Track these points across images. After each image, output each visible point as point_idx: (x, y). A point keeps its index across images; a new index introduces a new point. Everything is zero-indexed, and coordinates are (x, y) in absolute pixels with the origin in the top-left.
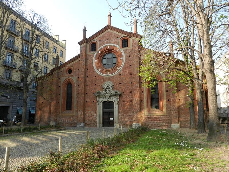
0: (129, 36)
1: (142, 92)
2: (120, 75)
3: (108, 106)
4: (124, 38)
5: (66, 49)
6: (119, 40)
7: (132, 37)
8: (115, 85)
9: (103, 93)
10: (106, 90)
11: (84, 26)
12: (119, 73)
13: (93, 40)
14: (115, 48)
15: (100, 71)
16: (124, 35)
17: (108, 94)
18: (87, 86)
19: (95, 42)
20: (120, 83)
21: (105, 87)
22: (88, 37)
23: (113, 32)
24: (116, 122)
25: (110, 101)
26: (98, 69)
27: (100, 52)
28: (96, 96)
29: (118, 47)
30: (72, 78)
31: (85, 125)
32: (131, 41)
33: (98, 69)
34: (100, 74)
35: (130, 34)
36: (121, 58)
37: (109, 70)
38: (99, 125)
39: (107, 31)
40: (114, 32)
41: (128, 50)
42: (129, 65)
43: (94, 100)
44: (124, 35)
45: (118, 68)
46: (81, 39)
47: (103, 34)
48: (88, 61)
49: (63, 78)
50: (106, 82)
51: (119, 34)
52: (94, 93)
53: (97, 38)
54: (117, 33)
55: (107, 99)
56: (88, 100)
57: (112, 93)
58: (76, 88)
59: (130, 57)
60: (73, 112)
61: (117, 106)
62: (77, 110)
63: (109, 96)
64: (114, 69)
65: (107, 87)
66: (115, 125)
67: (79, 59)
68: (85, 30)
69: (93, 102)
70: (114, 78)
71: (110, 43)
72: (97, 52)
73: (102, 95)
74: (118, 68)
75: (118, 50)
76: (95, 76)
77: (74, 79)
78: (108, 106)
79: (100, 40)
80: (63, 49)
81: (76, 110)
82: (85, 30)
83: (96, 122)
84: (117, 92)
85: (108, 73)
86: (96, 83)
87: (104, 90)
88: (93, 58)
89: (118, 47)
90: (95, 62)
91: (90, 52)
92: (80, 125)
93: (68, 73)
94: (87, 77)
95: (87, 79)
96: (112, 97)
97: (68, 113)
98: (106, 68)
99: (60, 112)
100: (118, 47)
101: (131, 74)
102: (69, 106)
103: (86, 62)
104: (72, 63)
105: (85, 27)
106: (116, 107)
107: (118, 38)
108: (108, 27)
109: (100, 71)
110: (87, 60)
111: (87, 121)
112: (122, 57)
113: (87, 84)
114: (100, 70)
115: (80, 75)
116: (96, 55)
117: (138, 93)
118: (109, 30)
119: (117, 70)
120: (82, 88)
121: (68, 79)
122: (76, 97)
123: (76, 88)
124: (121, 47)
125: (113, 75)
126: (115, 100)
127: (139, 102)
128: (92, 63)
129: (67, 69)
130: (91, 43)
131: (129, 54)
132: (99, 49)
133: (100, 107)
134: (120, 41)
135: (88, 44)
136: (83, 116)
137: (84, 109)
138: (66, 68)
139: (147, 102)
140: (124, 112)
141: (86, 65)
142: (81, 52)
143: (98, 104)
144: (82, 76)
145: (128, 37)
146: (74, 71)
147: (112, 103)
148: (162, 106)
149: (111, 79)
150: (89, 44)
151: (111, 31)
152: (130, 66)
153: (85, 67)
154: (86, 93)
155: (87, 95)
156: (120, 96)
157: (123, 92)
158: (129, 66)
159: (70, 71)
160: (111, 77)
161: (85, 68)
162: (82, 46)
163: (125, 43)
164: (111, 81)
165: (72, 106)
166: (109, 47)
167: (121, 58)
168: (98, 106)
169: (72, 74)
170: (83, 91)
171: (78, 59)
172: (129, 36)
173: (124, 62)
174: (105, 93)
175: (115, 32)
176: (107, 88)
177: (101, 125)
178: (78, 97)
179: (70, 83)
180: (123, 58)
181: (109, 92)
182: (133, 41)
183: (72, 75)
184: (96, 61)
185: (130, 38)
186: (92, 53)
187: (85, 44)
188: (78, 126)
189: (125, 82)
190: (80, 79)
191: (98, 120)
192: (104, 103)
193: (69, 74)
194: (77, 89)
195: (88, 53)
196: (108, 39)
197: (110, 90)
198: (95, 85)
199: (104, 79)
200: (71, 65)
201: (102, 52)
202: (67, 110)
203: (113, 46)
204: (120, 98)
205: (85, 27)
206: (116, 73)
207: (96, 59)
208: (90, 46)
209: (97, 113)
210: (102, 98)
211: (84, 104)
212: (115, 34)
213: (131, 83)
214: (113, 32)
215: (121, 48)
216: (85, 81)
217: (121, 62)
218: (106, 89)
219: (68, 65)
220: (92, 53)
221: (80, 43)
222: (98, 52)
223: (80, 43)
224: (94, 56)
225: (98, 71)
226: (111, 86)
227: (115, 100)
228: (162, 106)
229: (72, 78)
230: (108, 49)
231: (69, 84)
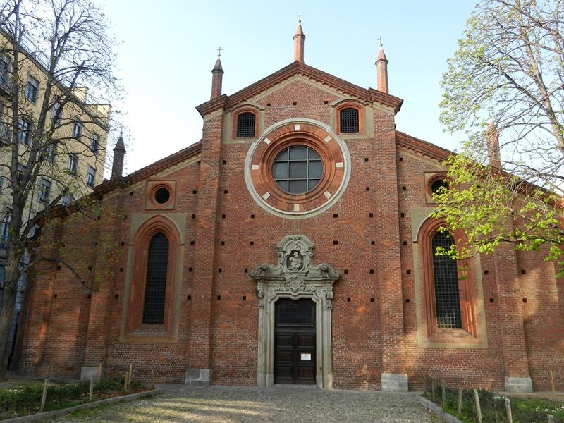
0: (363, 101)
1: (409, 272)
2: (336, 216)
3: (295, 313)
4: (346, 105)
6: (332, 109)
7: (374, 103)
8: (318, 250)
9: (279, 272)
10: (289, 263)
11: (217, 58)
12: (333, 208)
13: (242, 104)
14: (317, 133)
15: (269, 200)
16: (348, 97)
17: (297, 275)
18: (223, 247)
19: (254, 110)
20: (336, 243)
21: (285, 252)
22: (229, 89)
23: (311, 83)
24: (322, 369)
25: (301, 299)
26: (262, 194)
27: (268, 141)
28: (256, 282)
29: (328, 128)
30: (170, 216)
31: (214, 377)
32: (368, 115)
33: (262, 194)
34: (268, 210)
35: (370, 96)
36: (339, 165)
37: (300, 198)
38: (264, 377)
39: (291, 80)
40: (315, 85)
41: (360, 140)
42: (364, 188)
43: (248, 291)
44: (346, 95)
45: (327, 194)
46: (206, 96)
47: (278, 87)
48: (227, 165)
49: (136, 214)
50: (291, 236)
51: (333, 91)
52: (246, 271)
53: (257, 98)
54: (326, 88)
55: (294, 291)
56: (223, 292)
57: (307, 273)
58: (183, 249)
59: (368, 163)
60: (171, 333)
61: (327, 314)
62: (184, 324)
63: (298, 282)
64: (314, 198)
65: (293, 251)
66: (318, 377)
67: (195, 159)
68: (218, 71)
69: (244, 298)
70: (314, 226)
71: (303, 116)
72: (259, 140)
73: (276, 279)
74: (327, 194)
75: (327, 140)
76: (253, 216)
77: (177, 221)
78: (295, 313)
79: (269, 105)
80: (101, 132)
81: (181, 326)
82: (218, 71)
83: (251, 367)
84: (327, 271)
85: (297, 207)
87: (281, 260)
88: (244, 158)
90: (253, 172)
91: (234, 138)
92: (198, 376)
93: (156, 203)
94: (224, 216)
95: (225, 223)
96: (311, 287)
97: (152, 334)
98: (288, 192)
99: (122, 328)
100: (328, 131)
101: (371, 215)
102: (154, 309)
103: (221, 169)
104: (172, 168)
105: (219, 61)
106: (323, 318)
107: (326, 102)
108: (297, 68)
109: (269, 200)
110: (225, 162)
111: (220, 364)
112: (341, 160)
113: (224, 238)
114: (267, 195)
115: (199, 209)
116: (257, 151)
117: (397, 276)
118: (298, 77)
119: (325, 199)
120: (205, 251)
121: (155, 220)
122: (184, 283)
123: (183, 249)
124: (338, 129)
126: (321, 295)
127: (401, 303)
128: (242, 172)
129: (154, 188)
130: (240, 111)
131: (365, 154)
132: (266, 131)
133: (266, 319)
134: (333, 114)
135: (229, 114)
136: (206, 346)
137: (212, 323)
138: (151, 184)
139: (425, 305)
140: (347, 334)
141: (221, 179)
142: (204, 135)
143: (263, 307)
144: (206, 213)
145: (360, 102)
146: (180, 194)
147: (307, 306)
148: (473, 315)
149: (305, 226)
150: (233, 113)
151: (306, 80)
152: (368, 189)
153: (219, 184)
154: (220, 271)
155: (221, 275)
156: (336, 283)
157: (346, 272)
158: (363, 189)
159: (162, 194)
160: (304, 220)
161: (220, 189)
162: (208, 117)
163: (349, 120)
164: (306, 234)
165: (168, 310)
166: (297, 128)
167: (337, 164)
168: (261, 312)
169: (170, 204)
170: (211, 261)
171: (195, 158)
172: (363, 101)
173: (349, 177)
174: (285, 270)
175: (319, 86)
176: (292, 255)
177: (270, 378)
178: (189, 283)
179: (160, 233)
180: (346, 164)
181: (300, 269)
182: (376, 117)
183: (171, 207)
184: (256, 167)
185: (367, 107)
186: (242, 141)
187: (220, 112)
188: (189, 380)
189: (353, 241)
190: (203, 222)
191: (260, 362)
192: (283, 306)
194: (186, 256)
195: (229, 140)
196: (295, 104)
197: (302, 264)
198: (252, 244)
200: (168, 176)
201: (275, 142)
202: (145, 324)
203: (313, 125)
204: (336, 288)
205: (219, 61)
206: (322, 209)
207: (253, 162)
208: (234, 121)
209: (256, 337)
210: (273, 289)
211: (213, 305)
212: (318, 91)
213: (373, 243)
214: (313, 83)
215: (337, 134)
216: (218, 228)
217: (340, 177)
218: (291, 259)
219: (158, 174)
220: (242, 142)
221: (203, 110)
222: (262, 143)
223: (203, 110)
225: (261, 201)
226: (304, 248)
227: (321, 295)
228: (473, 315)
229: (170, 216)
230: (296, 134)
231: (159, 240)
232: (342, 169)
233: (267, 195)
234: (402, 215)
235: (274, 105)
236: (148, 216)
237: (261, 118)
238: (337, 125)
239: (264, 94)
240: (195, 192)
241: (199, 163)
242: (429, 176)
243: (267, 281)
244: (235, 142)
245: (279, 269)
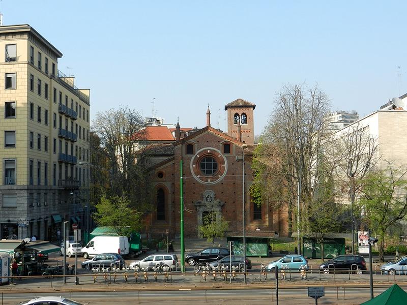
5: (89, 105)
10: (207, 200)
20: (222, 193)
28: (196, 206)
29: (220, 152)
36: (223, 165)
45: (220, 176)
53: (194, 139)
67: (172, 162)
71: (210, 147)
75: (219, 156)
77: (168, 185)
86: (194, 191)
89: (220, 152)
90: (193, 167)
100: (220, 152)
105: (178, 123)
123: (170, 195)
125: (214, 183)
128: (190, 168)
132: (198, 152)
134: (221, 146)
138: (156, 172)
149: (212, 187)
156: (223, 206)
158: (231, 173)
159: (161, 175)
166: (209, 151)
169: (164, 179)
174: (206, 202)
176: (208, 197)
180: (226, 165)
183: (165, 180)
184: (194, 166)
187: (180, 145)
193: (160, 179)
195: (184, 156)
199: (205, 187)
207: (193, 164)
222: (196, 156)
224: (192, 160)
230: (208, 153)
231: (161, 192)
233: (199, 176)
236: (157, 183)
237: (195, 147)
239: (196, 137)
240: (173, 175)
241: (174, 164)
243: (200, 206)
244: (186, 156)
245: (204, 202)
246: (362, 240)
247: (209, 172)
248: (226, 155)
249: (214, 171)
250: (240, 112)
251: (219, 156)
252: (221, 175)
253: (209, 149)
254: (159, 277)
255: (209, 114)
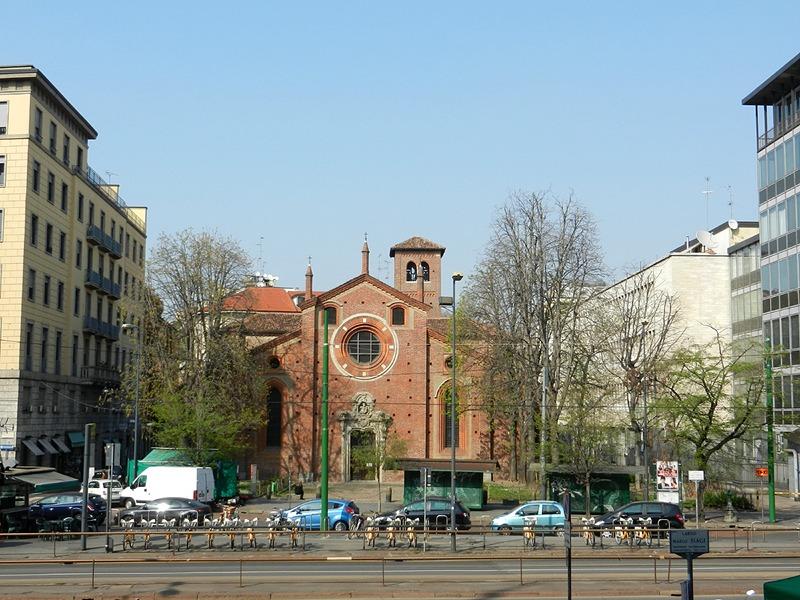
5: (145, 237)
10: (359, 410)
14: (378, 325)
27: (345, 329)
29: (384, 322)
32: (411, 313)
36: (391, 347)
45: (383, 366)
71: (368, 312)
73: (352, 420)
74: (383, 366)
85: (364, 374)
89: (384, 322)
90: (336, 350)
100: (384, 323)
114: (345, 366)
118: (365, 283)
119: (382, 369)
126: (378, 429)
132: (344, 322)
134: (389, 312)
149: (369, 386)
151: (370, 286)
158: (405, 364)
163: (398, 316)
166: (365, 321)
176: (361, 405)
180: (396, 346)
182: (416, 317)
184: (337, 347)
199: (360, 386)
225: (340, 369)
226: (369, 400)
232: (393, 350)
233: (345, 366)
234: (428, 381)
235: (349, 302)
237: (340, 312)
238: (390, 320)
242: (446, 356)
246: (663, 478)
247: (364, 359)
248: (398, 328)
249: (374, 357)
250: (416, 259)
251: (384, 329)
252: (387, 364)
253: (364, 316)
254: (279, 540)
255: (367, 252)
